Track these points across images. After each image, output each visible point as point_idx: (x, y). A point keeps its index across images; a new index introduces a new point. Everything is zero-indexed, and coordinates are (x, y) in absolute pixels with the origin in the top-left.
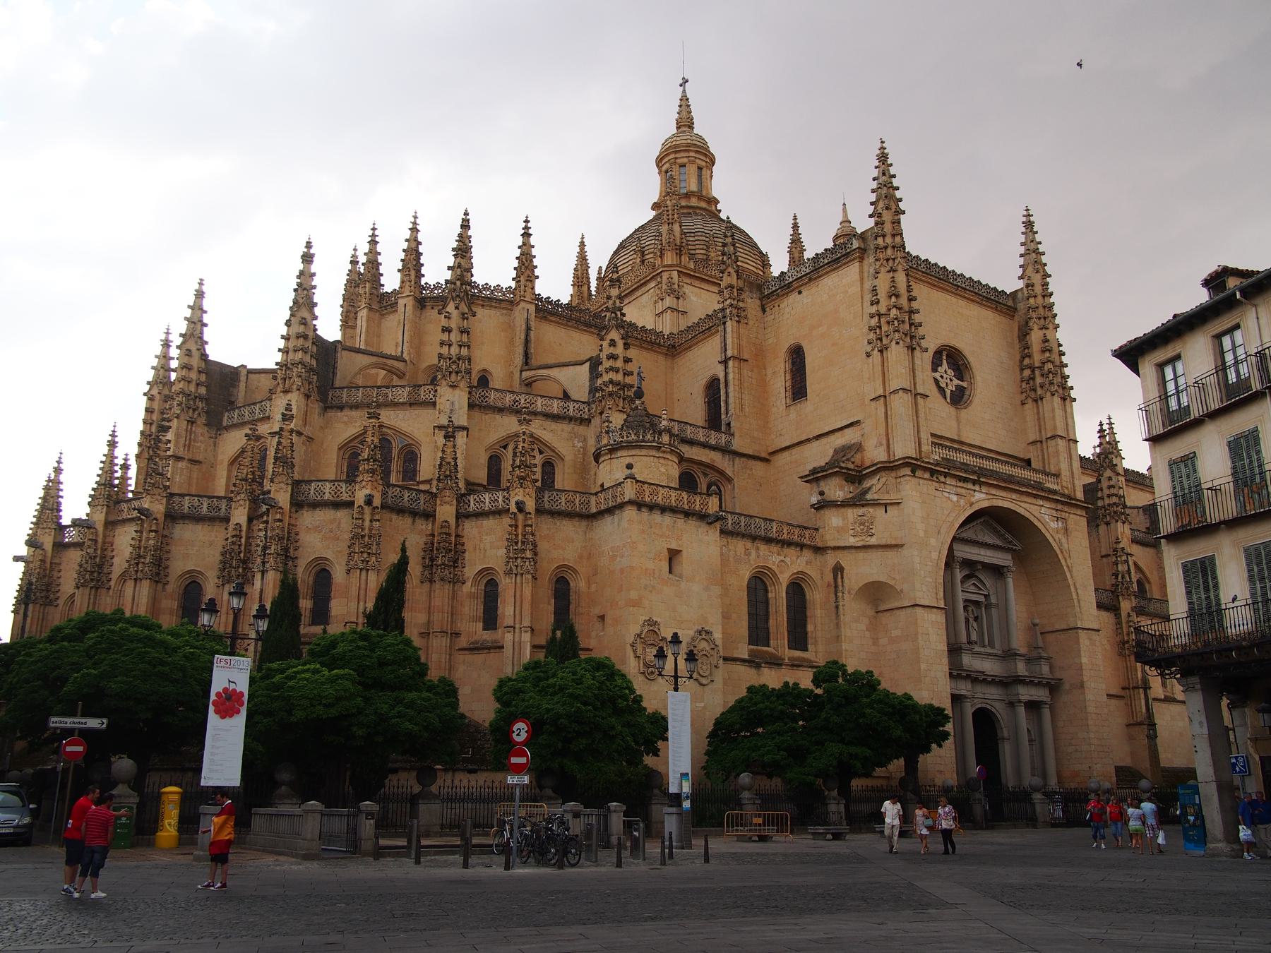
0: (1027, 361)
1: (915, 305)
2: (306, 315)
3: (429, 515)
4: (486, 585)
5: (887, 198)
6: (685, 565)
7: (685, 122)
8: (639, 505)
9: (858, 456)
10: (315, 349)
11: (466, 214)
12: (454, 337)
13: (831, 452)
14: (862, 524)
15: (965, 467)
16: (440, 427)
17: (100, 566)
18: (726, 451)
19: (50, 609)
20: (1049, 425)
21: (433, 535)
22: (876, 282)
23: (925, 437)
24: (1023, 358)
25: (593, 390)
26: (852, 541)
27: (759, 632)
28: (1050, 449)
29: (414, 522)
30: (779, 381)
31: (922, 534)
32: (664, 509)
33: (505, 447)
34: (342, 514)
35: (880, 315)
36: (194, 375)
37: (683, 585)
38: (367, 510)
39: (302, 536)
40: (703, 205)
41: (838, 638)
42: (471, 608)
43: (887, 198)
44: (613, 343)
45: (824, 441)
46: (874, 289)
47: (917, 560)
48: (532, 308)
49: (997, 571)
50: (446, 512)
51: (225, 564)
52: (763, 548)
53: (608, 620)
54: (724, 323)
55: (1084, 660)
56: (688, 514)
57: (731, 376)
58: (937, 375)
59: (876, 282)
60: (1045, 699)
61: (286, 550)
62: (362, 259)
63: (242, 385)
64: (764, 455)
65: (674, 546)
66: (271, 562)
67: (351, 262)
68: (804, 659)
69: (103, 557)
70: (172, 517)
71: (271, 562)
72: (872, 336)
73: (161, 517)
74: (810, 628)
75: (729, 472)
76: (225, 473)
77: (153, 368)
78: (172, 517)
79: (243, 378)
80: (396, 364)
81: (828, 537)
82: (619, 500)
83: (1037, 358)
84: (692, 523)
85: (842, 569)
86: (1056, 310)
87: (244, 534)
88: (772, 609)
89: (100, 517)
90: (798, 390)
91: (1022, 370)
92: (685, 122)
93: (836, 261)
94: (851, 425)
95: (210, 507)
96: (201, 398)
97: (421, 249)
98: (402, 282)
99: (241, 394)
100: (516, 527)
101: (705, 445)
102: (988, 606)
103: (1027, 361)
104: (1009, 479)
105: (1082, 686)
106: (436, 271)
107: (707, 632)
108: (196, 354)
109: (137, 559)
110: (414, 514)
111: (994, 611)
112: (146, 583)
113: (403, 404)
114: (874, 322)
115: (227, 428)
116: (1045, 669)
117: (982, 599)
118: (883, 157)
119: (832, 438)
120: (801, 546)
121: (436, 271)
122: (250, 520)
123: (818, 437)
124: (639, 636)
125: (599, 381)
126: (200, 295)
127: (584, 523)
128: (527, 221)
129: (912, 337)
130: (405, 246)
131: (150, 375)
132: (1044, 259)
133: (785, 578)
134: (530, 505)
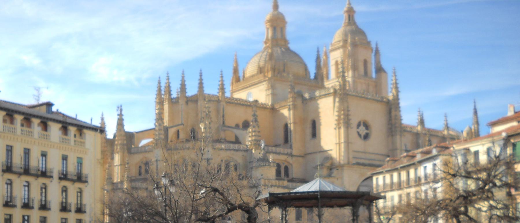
1: (350, 113)
11: (201, 70)
16: (205, 159)
18: (291, 155)
23: (351, 157)
30: (309, 131)
33: (222, 161)
58: (359, 130)
62: (163, 85)
75: (291, 162)
79: (135, 136)
93: (326, 95)
101: (283, 154)
106: (192, 91)
115: (133, 153)
128: (222, 72)
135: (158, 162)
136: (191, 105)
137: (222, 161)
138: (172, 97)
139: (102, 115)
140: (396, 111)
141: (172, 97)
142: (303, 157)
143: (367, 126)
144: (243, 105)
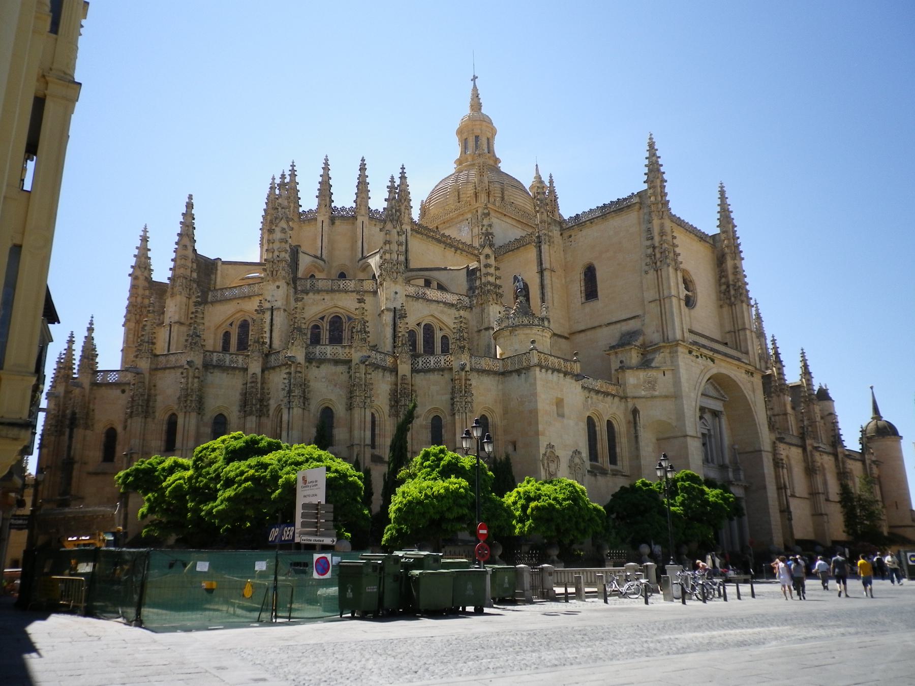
0: (723, 280)
1: (675, 241)
2: (285, 226)
3: (394, 370)
4: (433, 419)
5: (654, 172)
6: (566, 411)
7: (476, 105)
8: (541, 367)
9: (641, 338)
10: (288, 249)
11: (363, 160)
12: (394, 247)
13: (618, 335)
14: (649, 382)
15: (704, 347)
16: (388, 310)
17: (148, 401)
19: (89, 433)
20: (740, 322)
21: (396, 385)
22: (650, 226)
24: (721, 277)
25: (472, 289)
26: (643, 393)
27: (593, 455)
28: (741, 337)
30: (578, 287)
31: (687, 390)
32: (554, 370)
34: (341, 368)
35: (654, 248)
36: (190, 265)
37: (565, 421)
38: (362, 367)
39: (311, 384)
40: (491, 162)
41: (638, 457)
43: (654, 172)
44: (487, 256)
45: (612, 327)
46: (649, 230)
47: (685, 406)
48: (409, 228)
49: (715, 414)
50: (404, 368)
51: (245, 404)
52: (595, 397)
53: (519, 445)
54: (540, 247)
55: (766, 471)
56: (566, 374)
57: (547, 281)
59: (650, 226)
60: (742, 496)
61: (304, 392)
63: (219, 272)
64: (566, 335)
65: (559, 396)
66: (296, 402)
67: (271, 188)
68: (617, 471)
69: (149, 395)
70: (208, 366)
71: (296, 402)
72: (648, 260)
73: (200, 366)
74: (618, 450)
76: (212, 336)
77: (135, 256)
78: (208, 366)
79: (219, 268)
80: (319, 261)
81: (628, 391)
82: (524, 364)
83: (731, 277)
84: (568, 380)
85: (639, 412)
86: (741, 248)
87: (259, 380)
88: (599, 437)
89: (144, 365)
90: (591, 292)
91: (720, 285)
92: (476, 105)
94: (634, 318)
95: (231, 361)
96: (194, 281)
97: (331, 182)
98: (319, 205)
99: (220, 280)
100: (460, 379)
102: (710, 436)
103: (723, 280)
104: (726, 355)
105: (765, 488)
106: (344, 198)
107: (579, 453)
108: (190, 249)
109: (185, 397)
110: (385, 369)
111: (713, 440)
112: (194, 415)
113: (352, 292)
114: (650, 251)
115: (212, 303)
116: (742, 477)
117: (706, 432)
118: (651, 146)
119: (618, 326)
120: (614, 396)
121: (344, 198)
122: (263, 371)
123: (609, 324)
124: (545, 455)
125: (478, 283)
126: (190, 206)
127: (497, 378)
128: (403, 168)
129: (676, 263)
130: (320, 179)
131: (133, 261)
132: (732, 215)
133: (606, 419)
134: (468, 368)
135: (275, 313)
136: (341, 227)
137: (418, 325)
138: (301, 210)
139: (145, 231)
140: (734, 259)
141: (301, 210)
142: (566, 338)
143: (688, 283)
144: (439, 241)
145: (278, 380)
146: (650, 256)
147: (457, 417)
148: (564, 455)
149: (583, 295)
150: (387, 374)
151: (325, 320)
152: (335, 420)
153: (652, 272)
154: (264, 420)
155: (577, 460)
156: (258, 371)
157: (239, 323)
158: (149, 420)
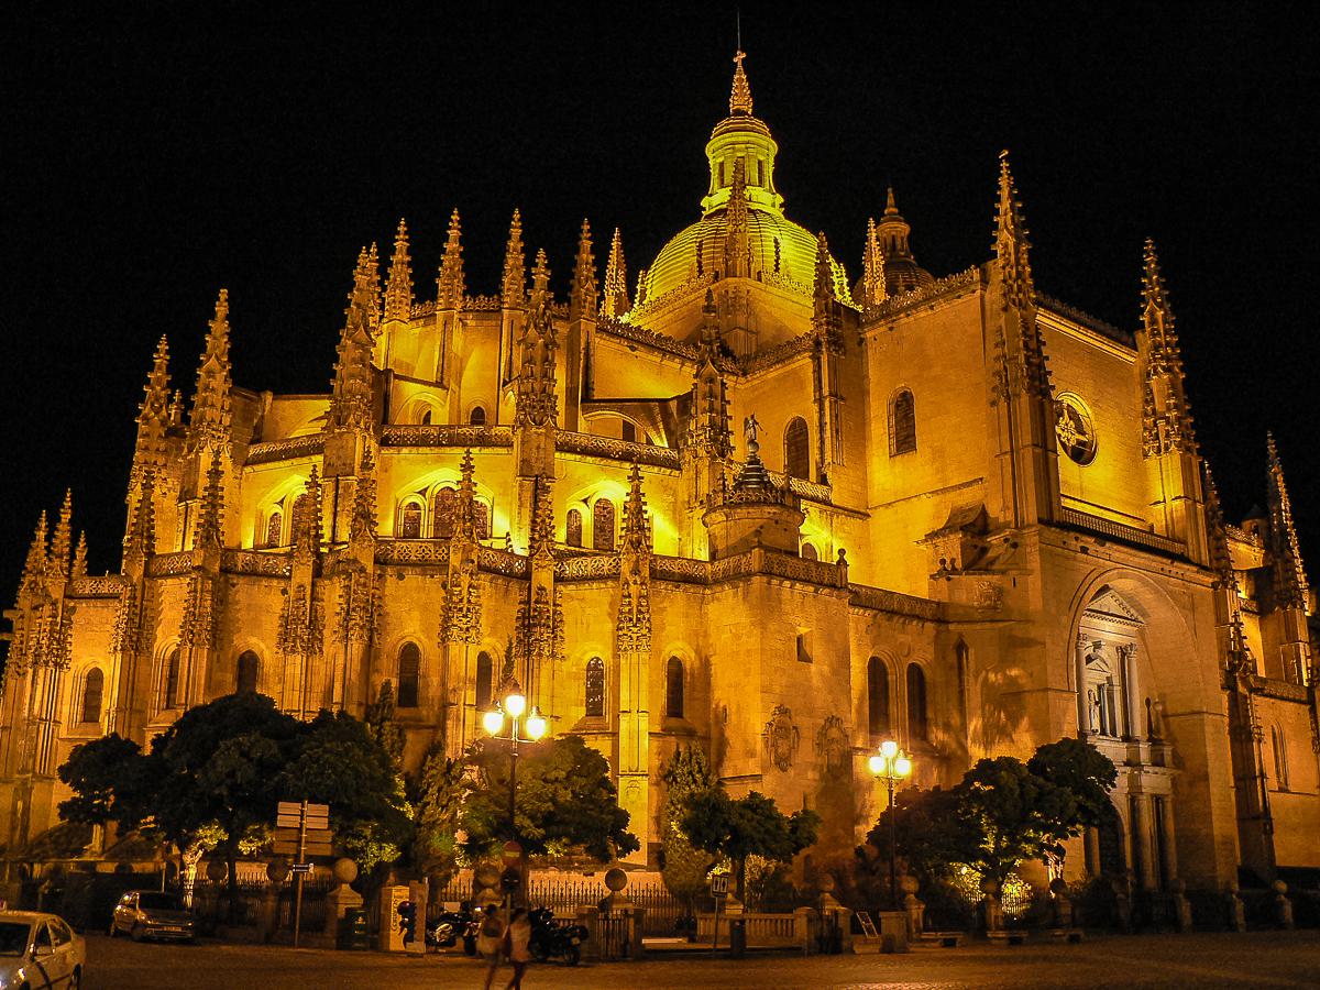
29: (507, 591)
42: (578, 690)
50: (543, 577)
55: (1210, 750)
105: (1206, 777)
116: (1168, 758)
145: (333, 594)
146: (997, 373)
147: (623, 661)
148: (807, 725)
149: (893, 441)
150: (515, 586)
151: (429, 491)
152: (422, 664)
153: (1003, 404)
154: (317, 662)
155: (834, 733)
156: (307, 580)
157: (294, 499)
158: (141, 659)
